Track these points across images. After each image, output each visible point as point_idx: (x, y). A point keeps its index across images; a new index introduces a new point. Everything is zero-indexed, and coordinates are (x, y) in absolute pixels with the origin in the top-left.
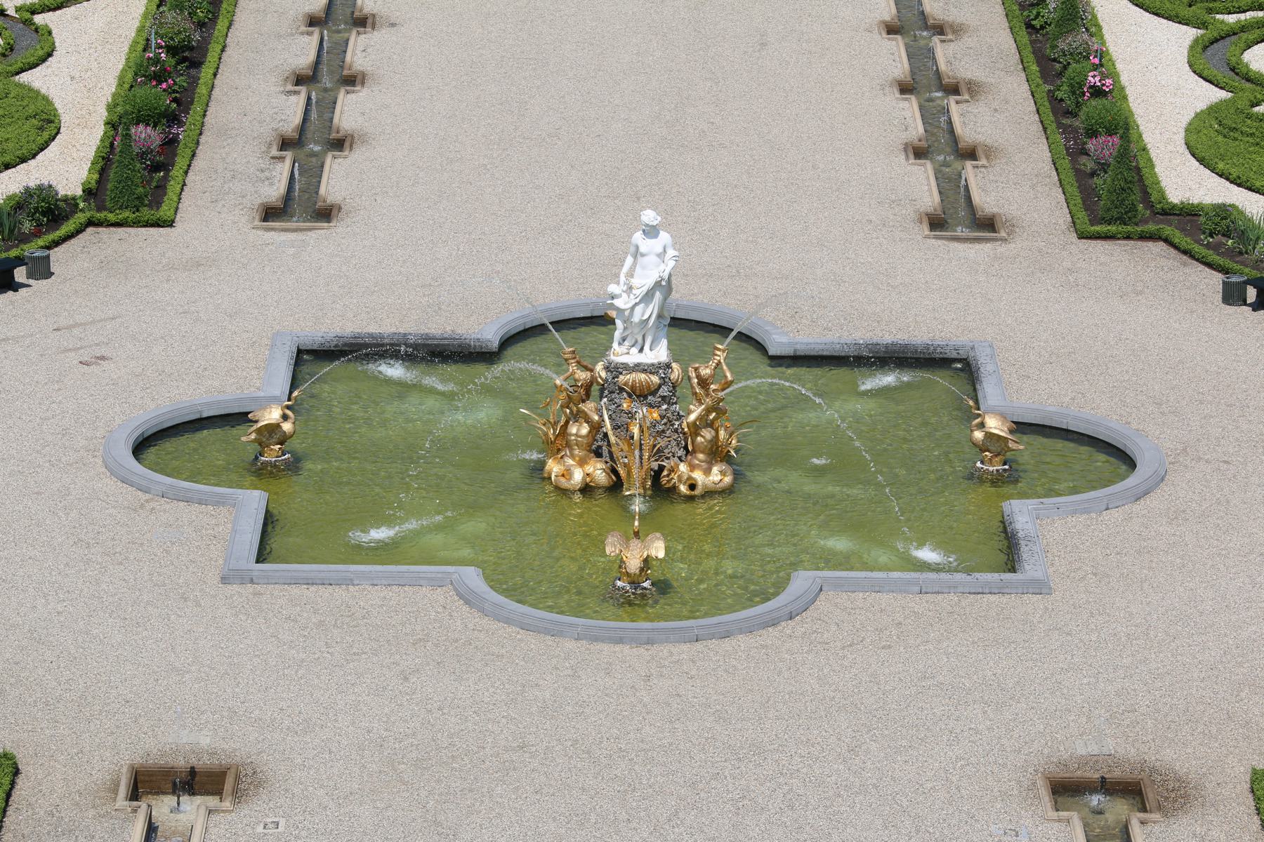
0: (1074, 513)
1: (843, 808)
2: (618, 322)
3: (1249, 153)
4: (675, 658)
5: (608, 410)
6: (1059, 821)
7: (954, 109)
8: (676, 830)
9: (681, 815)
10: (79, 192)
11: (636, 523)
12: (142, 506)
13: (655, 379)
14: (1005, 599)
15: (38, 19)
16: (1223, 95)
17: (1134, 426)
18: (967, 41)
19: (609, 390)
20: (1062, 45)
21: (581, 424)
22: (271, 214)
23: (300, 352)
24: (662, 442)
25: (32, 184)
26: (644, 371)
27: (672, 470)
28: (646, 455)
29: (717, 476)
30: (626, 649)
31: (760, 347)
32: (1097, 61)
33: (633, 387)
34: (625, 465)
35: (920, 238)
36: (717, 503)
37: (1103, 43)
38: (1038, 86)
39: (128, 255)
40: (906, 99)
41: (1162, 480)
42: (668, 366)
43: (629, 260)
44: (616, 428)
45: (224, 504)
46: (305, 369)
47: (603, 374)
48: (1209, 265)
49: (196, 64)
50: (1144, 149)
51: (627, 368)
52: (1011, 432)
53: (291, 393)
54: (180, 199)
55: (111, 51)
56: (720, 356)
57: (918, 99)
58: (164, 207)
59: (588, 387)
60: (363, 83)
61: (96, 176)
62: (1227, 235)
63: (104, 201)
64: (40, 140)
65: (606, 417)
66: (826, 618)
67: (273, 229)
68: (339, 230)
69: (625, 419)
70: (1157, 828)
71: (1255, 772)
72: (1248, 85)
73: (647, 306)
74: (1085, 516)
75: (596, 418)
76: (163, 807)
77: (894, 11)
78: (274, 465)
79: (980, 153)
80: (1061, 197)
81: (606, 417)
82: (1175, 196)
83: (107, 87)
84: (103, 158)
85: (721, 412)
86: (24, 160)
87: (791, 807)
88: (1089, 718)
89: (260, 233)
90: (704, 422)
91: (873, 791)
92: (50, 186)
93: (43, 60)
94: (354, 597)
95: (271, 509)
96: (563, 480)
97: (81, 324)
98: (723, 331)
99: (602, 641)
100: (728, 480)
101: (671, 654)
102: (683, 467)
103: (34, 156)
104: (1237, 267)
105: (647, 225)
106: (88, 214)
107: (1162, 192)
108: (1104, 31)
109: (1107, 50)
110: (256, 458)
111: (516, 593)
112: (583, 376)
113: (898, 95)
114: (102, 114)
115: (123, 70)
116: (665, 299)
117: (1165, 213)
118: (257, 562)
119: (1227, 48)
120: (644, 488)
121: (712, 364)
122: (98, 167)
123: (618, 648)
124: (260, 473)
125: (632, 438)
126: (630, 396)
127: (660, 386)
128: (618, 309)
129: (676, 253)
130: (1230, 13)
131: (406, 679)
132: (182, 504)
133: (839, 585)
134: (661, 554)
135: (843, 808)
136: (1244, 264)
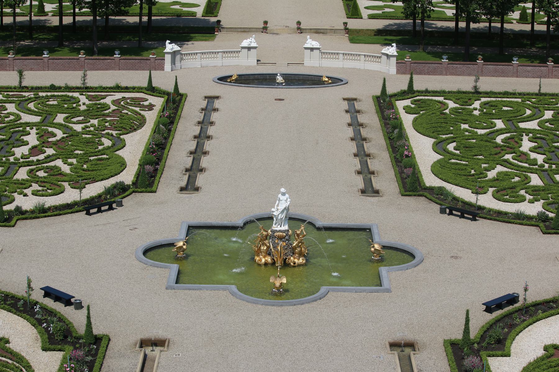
0: (398, 270)
1: (333, 351)
2: (275, 219)
3: (448, 173)
4: (289, 310)
5: (272, 243)
6: (392, 354)
7: (368, 160)
8: (287, 357)
9: (289, 353)
10: (131, 183)
11: (278, 273)
12: (145, 268)
13: (284, 234)
14: (379, 294)
15: (122, 137)
16: (441, 157)
17: (415, 247)
18: (373, 142)
19: (272, 237)
20: (398, 143)
21: (264, 247)
22: (182, 189)
23: (189, 227)
24: (286, 251)
25: (118, 181)
26: (281, 232)
27: (289, 259)
28: (282, 255)
29: (301, 260)
30: (275, 307)
31: (314, 225)
32: (407, 148)
33: (278, 236)
34: (276, 257)
35: (358, 196)
36: (301, 268)
37: (409, 142)
38: (391, 154)
39: (144, 200)
40: (356, 158)
41: (422, 261)
42: (288, 231)
43: (277, 202)
44: (274, 247)
45: (167, 268)
46: (191, 231)
47: (270, 233)
48: (437, 203)
49: (164, 149)
50: (420, 172)
51: (277, 231)
52: (381, 248)
53: (186, 237)
54: (158, 185)
55: (141, 145)
56: (303, 228)
57: (359, 158)
58: (154, 187)
59: (267, 236)
60: (208, 154)
61: (136, 179)
62: (441, 195)
63: (137, 186)
64: (121, 169)
65: (271, 245)
66: (330, 299)
67: (183, 193)
68: (201, 193)
69: (276, 245)
70: (418, 356)
71: (445, 340)
72: (448, 154)
73: (282, 215)
74: (401, 271)
75: (268, 245)
76: (148, 350)
77: (353, 134)
78: (181, 257)
79: (376, 173)
80: (397, 185)
81: (271, 245)
82: (428, 184)
83: (139, 155)
84: (138, 174)
85: (302, 243)
86: (116, 175)
87: (319, 351)
88: (400, 326)
89: (179, 194)
90: (298, 246)
91: (341, 346)
92: (123, 182)
93: (123, 148)
94: (202, 293)
95: (181, 268)
96: (259, 262)
97: (130, 219)
98: (303, 221)
99: (269, 305)
100: (304, 261)
101: (287, 309)
102: (292, 258)
103: (119, 174)
104: (444, 203)
105: (282, 192)
106: (133, 189)
107: (424, 183)
108: (410, 140)
109: (410, 146)
110: (176, 256)
111: (245, 292)
112: (265, 233)
113: (353, 157)
114: (138, 162)
115: (144, 150)
116: (287, 212)
117: (425, 189)
118: (176, 283)
119: (444, 144)
120: (282, 264)
121: (300, 230)
122: (136, 176)
123: (273, 307)
124: (177, 259)
125: (278, 250)
126: (278, 239)
127: (286, 236)
128: (274, 215)
129: (290, 200)
130: (443, 135)
131: (215, 316)
132: (156, 268)
133: (334, 290)
134: (285, 282)
135: (333, 351)
136: (445, 203)
